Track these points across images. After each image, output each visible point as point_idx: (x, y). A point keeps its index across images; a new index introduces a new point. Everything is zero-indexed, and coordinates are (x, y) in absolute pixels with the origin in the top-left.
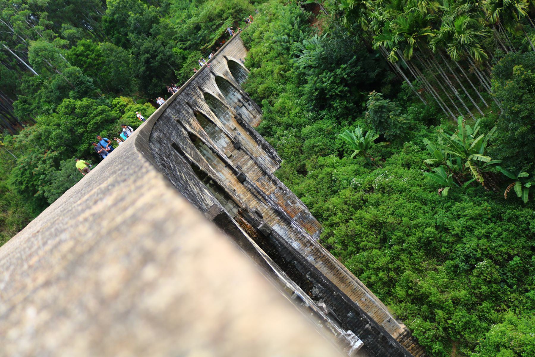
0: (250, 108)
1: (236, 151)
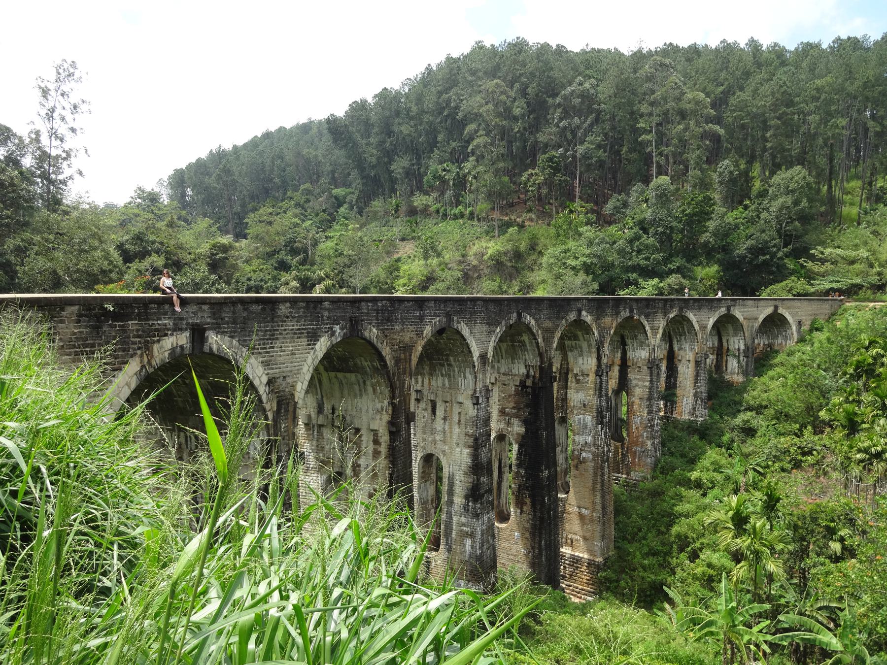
1: (646, 368)
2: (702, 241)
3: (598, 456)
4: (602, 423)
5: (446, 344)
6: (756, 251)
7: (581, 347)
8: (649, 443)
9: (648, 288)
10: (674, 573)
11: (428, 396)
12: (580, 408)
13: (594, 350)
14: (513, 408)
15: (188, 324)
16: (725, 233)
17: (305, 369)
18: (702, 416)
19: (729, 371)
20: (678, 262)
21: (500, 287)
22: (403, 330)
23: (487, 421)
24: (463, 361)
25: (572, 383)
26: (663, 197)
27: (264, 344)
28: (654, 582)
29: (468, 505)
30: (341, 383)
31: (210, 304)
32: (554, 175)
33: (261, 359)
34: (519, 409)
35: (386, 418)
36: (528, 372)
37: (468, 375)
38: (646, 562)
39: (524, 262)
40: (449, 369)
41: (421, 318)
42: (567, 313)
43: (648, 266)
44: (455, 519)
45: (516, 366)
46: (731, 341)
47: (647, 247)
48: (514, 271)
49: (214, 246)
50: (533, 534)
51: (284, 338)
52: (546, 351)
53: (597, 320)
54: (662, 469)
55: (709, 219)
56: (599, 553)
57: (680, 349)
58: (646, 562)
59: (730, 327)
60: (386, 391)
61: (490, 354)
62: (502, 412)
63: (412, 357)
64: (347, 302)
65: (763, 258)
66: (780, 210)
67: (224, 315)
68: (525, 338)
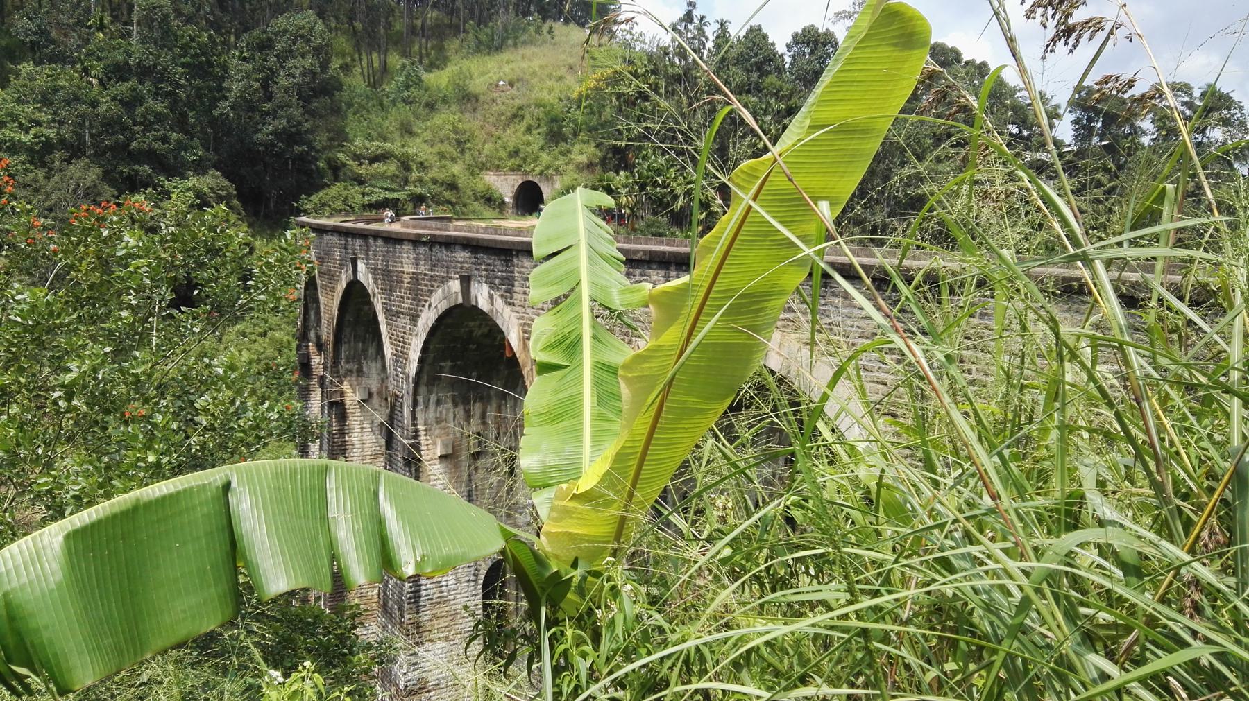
47: (159, 117)
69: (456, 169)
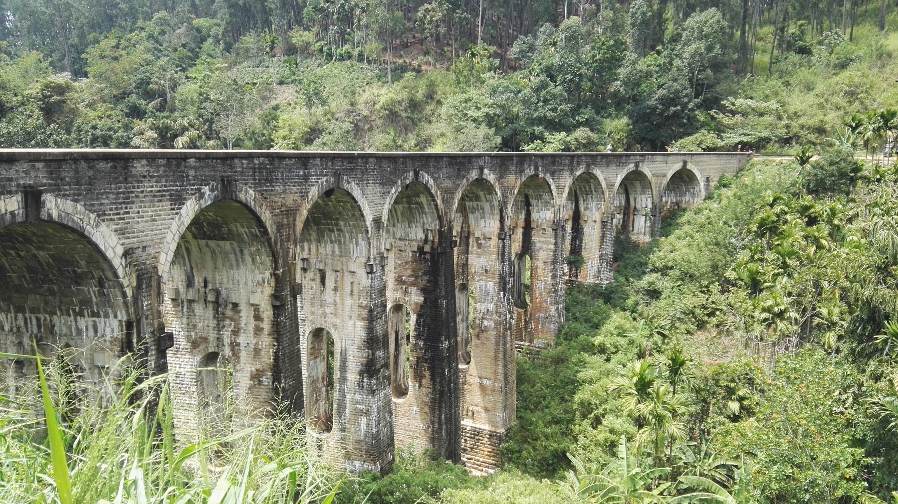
0: (648, 224)
1: (550, 230)
2: (612, 90)
3: (500, 324)
4: (504, 289)
5: (335, 208)
6: (667, 102)
7: (483, 209)
8: (553, 309)
9: (554, 143)
10: (577, 441)
11: (315, 264)
12: (481, 274)
13: (497, 211)
14: (411, 276)
15: (18, 185)
16: (634, 82)
17: (169, 237)
18: (607, 279)
19: (635, 231)
20: (587, 113)
21: (394, 141)
22: (284, 191)
23: (382, 291)
24: (354, 226)
25: (473, 248)
26: (573, 39)
27: (117, 209)
28: (557, 451)
29: (363, 381)
30: (213, 252)
31: (45, 161)
32: (454, 11)
33: (114, 227)
34: (417, 277)
35: (268, 290)
36: (426, 236)
37: (360, 241)
38: (549, 430)
39: (421, 112)
40: (339, 235)
41: (306, 178)
42: (468, 171)
43: (555, 118)
44: (349, 397)
45: (413, 230)
46: (639, 200)
47: (554, 96)
48: (410, 123)
49: (47, 86)
50: (432, 409)
51: (142, 202)
52: (446, 214)
53: (500, 178)
54: (565, 335)
55: (620, 66)
56: (501, 423)
57: (586, 209)
58: (549, 430)
59: (638, 185)
60: (268, 261)
61: (385, 218)
62: (399, 281)
63: (297, 223)
64: (217, 158)
65: (674, 109)
66: (692, 57)
67: (63, 174)
68: (423, 199)
69: (832, 118)
